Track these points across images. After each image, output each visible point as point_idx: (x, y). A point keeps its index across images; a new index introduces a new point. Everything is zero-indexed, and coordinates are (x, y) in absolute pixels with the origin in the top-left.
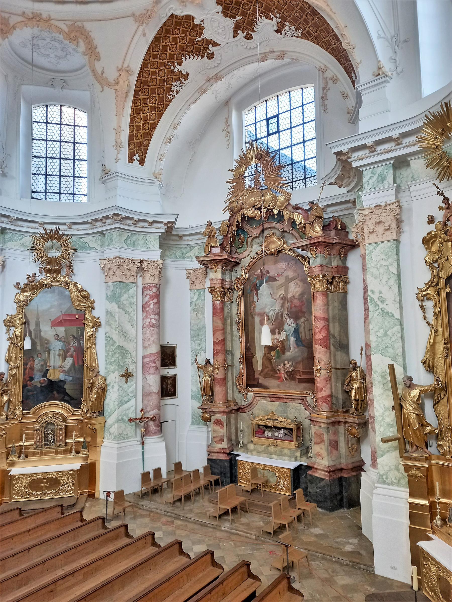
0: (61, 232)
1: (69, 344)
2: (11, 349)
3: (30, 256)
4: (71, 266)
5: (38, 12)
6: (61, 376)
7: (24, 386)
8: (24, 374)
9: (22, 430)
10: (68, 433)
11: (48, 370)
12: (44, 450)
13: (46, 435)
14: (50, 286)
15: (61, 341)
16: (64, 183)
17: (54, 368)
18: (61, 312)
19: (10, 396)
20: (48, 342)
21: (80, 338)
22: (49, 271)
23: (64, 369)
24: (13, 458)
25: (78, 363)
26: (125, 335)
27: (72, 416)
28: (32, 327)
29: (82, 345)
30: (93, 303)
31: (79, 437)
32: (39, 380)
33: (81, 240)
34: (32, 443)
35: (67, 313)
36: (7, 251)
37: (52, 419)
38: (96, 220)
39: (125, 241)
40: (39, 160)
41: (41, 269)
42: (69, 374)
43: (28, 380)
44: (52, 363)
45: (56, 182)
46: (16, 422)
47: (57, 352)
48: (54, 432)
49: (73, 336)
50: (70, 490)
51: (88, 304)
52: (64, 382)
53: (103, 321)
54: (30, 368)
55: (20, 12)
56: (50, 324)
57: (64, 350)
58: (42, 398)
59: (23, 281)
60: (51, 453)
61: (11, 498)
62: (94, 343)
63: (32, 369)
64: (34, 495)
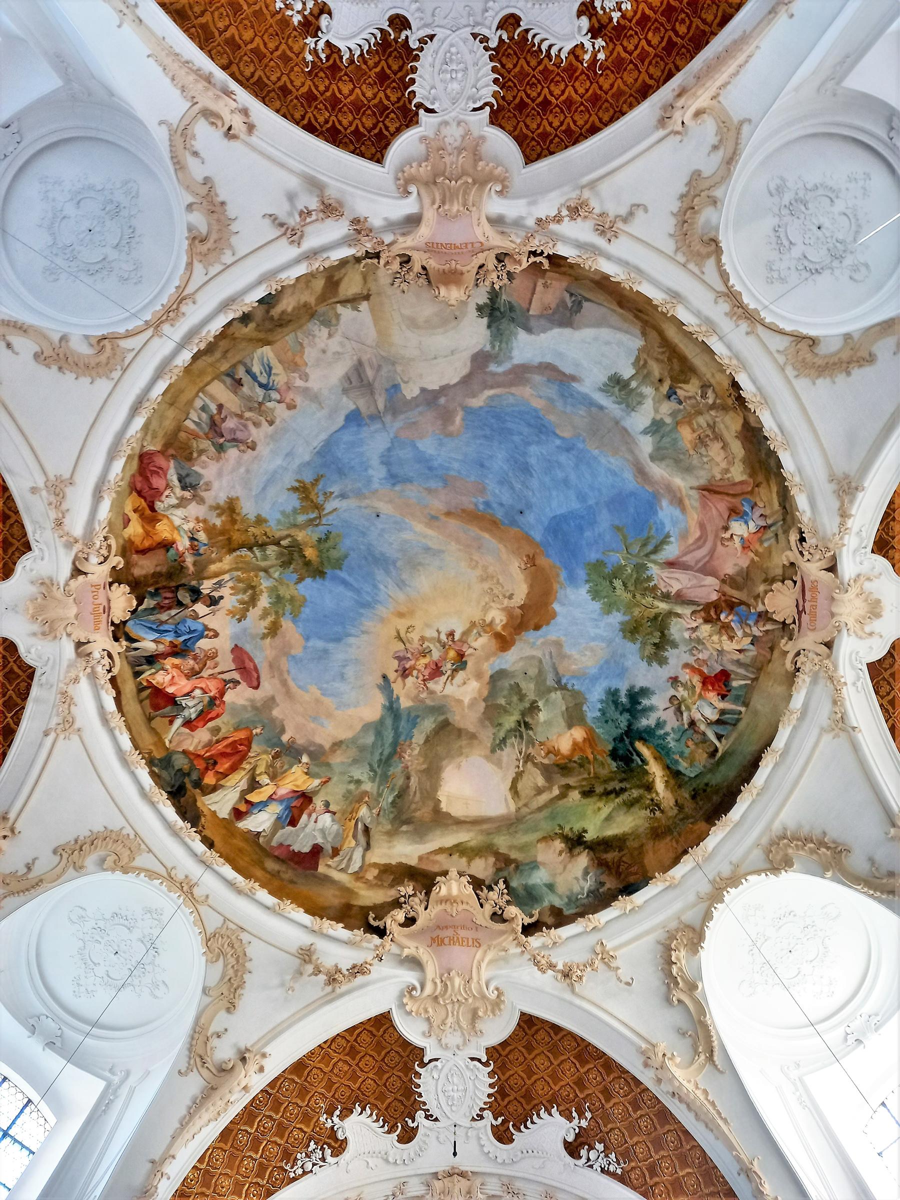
5: (178, 324)
55: (199, 297)
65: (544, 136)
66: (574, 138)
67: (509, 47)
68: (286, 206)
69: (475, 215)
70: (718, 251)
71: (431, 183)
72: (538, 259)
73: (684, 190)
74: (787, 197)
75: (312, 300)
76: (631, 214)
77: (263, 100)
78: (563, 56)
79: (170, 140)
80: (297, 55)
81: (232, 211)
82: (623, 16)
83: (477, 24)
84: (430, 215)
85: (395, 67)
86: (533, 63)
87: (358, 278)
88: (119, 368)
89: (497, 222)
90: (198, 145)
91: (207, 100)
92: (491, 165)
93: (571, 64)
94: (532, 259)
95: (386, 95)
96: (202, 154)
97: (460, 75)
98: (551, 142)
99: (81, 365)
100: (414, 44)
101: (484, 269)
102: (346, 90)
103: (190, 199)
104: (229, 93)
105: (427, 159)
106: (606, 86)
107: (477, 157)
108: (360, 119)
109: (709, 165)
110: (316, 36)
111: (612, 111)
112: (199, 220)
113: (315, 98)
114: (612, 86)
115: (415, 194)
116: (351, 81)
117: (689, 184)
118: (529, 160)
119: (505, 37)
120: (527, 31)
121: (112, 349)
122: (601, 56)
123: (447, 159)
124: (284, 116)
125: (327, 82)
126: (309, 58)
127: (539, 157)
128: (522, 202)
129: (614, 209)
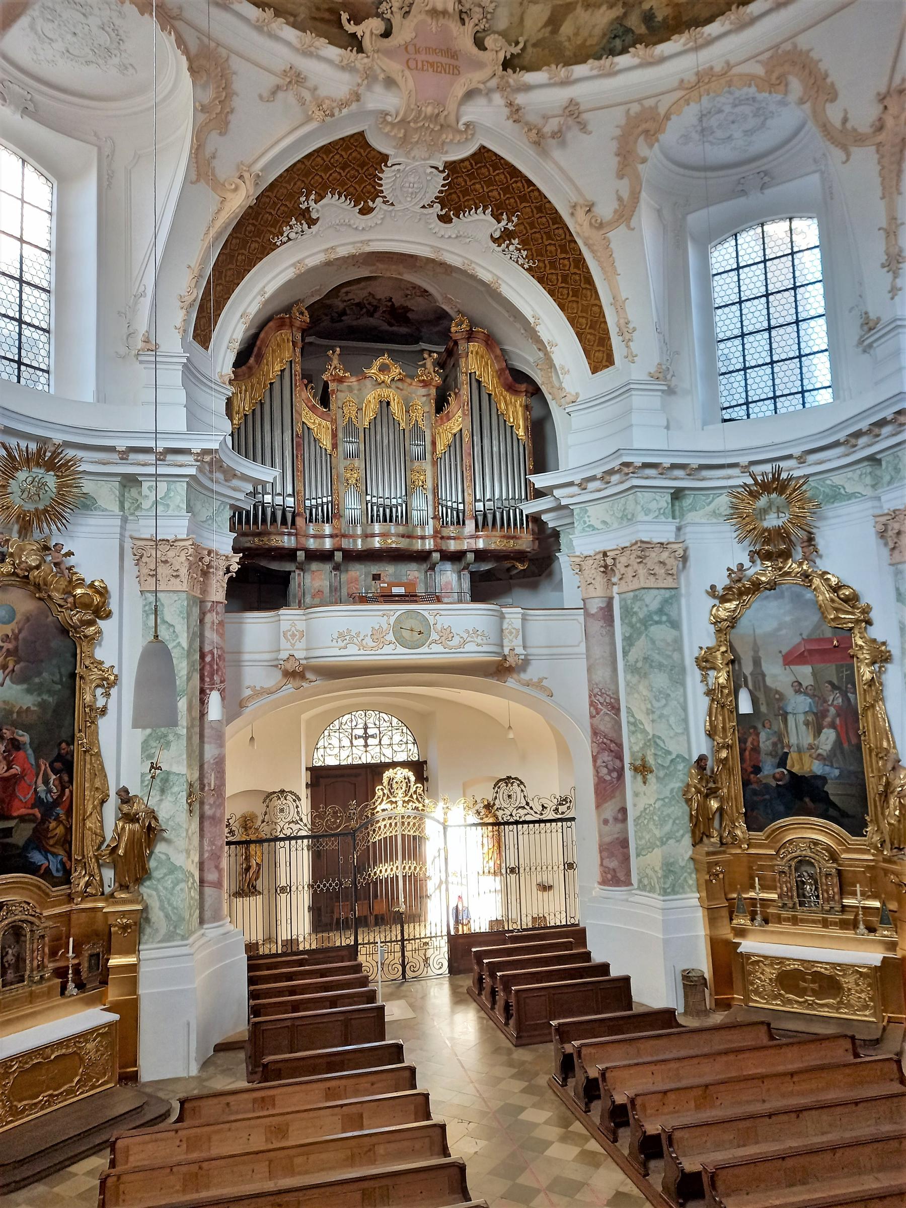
0: (784, 476)
1: (825, 701)
2: (714, 711)
3: (728, 533)
4: (810, 540)
6: (817, 768)
7: (746, 783)
8: (742, 760)
9: (751, 868)
10: (844, 886)
11: (786, 754)
12: (800, 915)
13: (800, 885)
14: (773, 586)
15: (806, 694)
16: (781, 375)
18: (801, 634)
19: (722, 800)
20: (782, 697)
21: (846, 687)
22: (768, 556)
23: (820, 751)
24: (742, 921)
25: (849, 742)
27: (848, 850)
28: (747, 669)
29: (852, 700)
30: (866, 610)
31: (868, 897)
32: (772, 772)
33: (828, 482)
34: (774, 896)
35: (814, 637)
36: (688, 529)
38: (858, 434)
40: (729, 344)
41: (752, 554)
42: (832, 763)
43: (752, 773)
44: (793, 740)
45: (765, 378)
46: (739, 851)
47: (801, 718)
48: (816, 883)
49: (831, 683)
50: (866, 1007)
51: (858, 615)
52: (823, 779)
53: (894, 648)
54: (752, 749)
56: (781, 661)
57: (815, 714)
58: (781, 808)
59: (722, 582)
60: (814, 922)
61: (747, 999)
62: (879, 697)
63: (756, 749)
64: (790, 1001)
66: (325, 149)
67: (368, 198)
68: (569, 136)
69: (413, 100)
70: (191, 69)
72: (351, 28)
73: (230, 117)
75: (579, 10)
76: (274, 93)
79: (632, 215)
80: (522, 223)
81: (614, 146)
82: (288, 224)
83: (390, 211)
84: (452, 106)
85: (454, 196)
86: (351, 189)
87: (528, 22)
88: (780, 51)
89: (390, 82)
90: (615, 205)
91: (596, 236)
92: (393, 134)
93: (324, 191)
94: (358, 30)
95: (466, 182)
98: (341, 146)
99: (807, 71)
100: (437, 206)
101: (404, 10)
102: (495, 193)
103: (640, 167)
104: (578, 233)
105: (443, 143)
108: (490, 174)
109: (214, 141)
112: (642, 149)
113: (519, 197)
115: (461, 123)
116: (489, 197)
117: (227, 123)
119: (370, 203)
120: (355, 206)
121: (773, 72)
122: (303, 199)
124: (546, 198)
125: (507, 202)
126: (515, 219)
129: (289, 97)
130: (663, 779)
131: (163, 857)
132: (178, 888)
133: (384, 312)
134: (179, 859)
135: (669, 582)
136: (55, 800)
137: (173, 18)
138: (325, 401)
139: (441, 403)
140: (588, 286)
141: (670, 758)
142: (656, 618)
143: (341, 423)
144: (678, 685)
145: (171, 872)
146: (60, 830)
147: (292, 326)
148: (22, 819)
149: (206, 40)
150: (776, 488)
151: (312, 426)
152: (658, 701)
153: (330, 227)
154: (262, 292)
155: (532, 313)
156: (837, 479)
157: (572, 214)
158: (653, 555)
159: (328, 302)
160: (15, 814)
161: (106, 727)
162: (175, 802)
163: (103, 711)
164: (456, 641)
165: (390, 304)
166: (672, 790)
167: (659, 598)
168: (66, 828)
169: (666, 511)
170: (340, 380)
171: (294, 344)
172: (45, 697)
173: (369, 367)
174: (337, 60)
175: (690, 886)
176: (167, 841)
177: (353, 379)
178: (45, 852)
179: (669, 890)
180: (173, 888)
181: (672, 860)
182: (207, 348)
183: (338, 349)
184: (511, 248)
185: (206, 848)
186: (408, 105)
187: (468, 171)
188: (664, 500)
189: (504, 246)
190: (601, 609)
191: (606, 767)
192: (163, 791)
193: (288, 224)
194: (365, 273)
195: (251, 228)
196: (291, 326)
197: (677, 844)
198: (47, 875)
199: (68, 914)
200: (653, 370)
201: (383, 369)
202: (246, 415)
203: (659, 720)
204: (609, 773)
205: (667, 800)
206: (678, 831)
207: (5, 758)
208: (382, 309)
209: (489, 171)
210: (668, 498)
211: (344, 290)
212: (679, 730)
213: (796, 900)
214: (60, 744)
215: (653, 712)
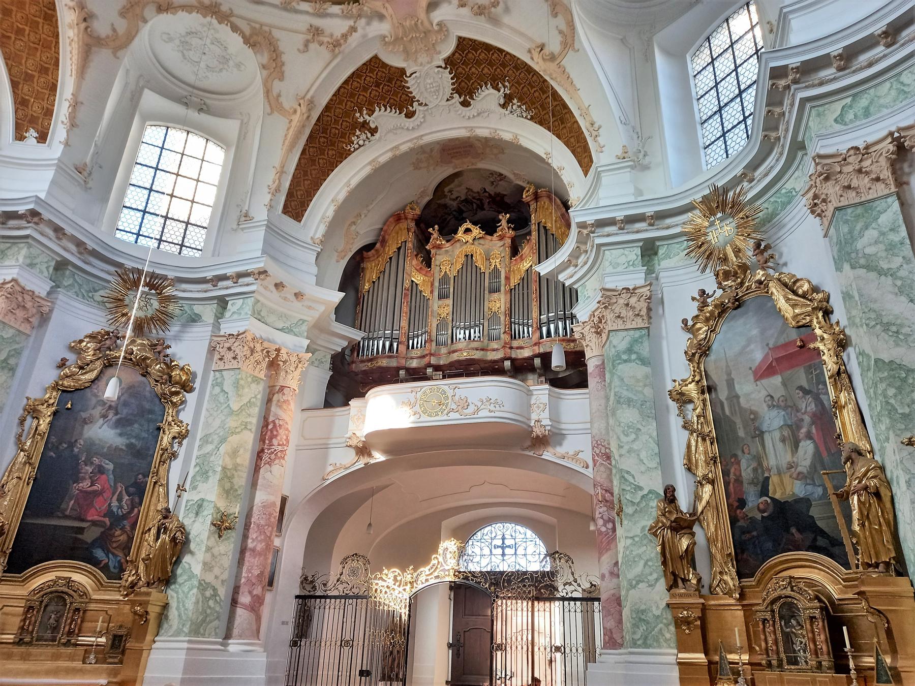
1: (798, 411)
6: (797, 489)
7: (734, 521)
15: (778, 407)
17: (779, 473)
18: (767, 345)
21: (818, 389)
22: (727, 275)
25: (828, 450)
26: (894, 329)
35: (779, 343)
36: (661, 275)
37: (788, 592)
39: (840, 120)
42: (813, 480)
43: (738, 507)
44: (772, 462)
47: (777, 435)
49: (801, 388)
56: (751, 377)
57: (790, 426)
58: (769, 545)
63: (739, 480)
65: (371, 71)
69: (395, 21)
71: (427, 33)
73: (284, 68)
74: (231, 63)
77: (526, 64)
78: (377, 109)
79: (574, 40)
80: (513, 85)
82: (354, 134)
83: (427, 110)
84: (422, 15)
85: (463, 84)
86: (392, 101)
89: (381, 17)
91: (552, 66)
96: (557, 32)
97: (428, 86)
98: (367, 69)
102: (486, 70)
105: (433, 45)
106: (349, 103)
107: (406, 52)
109: (277, 86)
110: (505, 94)
111: (340, 93)
114: (346, 105)
117: (283, 73)
118: (376, 57)
119: (411, 108)
120: (400, 113)
122: (358, 115)
123: (422, 46)
124: (515, 56)
126: (507, 84)
127: (370, 60)
128: (370, 35)
130: (633, 515)
131: (187, 566)
132: (191, 593)
133: (489, 203)
134: (197, 569)
135: (639, 323)
136: (124, 515)
137: (228, 16)
138: (429, 265)
139: (515, 251)
140: (566, 111)
141: (640, 493)
142: (625, 357)
143: (437, 277)
144: (650, 420)
145: (190, 579)
146: (123, 538)
147: (406, 219)
148: (94, 523)
149: (253, 24)
150: (717, 207)
151: (418, 283)
152: (627, 435)
153: (388, 132)
154: (348, 184)
155: (544, 151)
156: (789, 186)
157: (532, 59)
158: (621, 301)
159: (442, 201)
160: (89, 519)
161: (176, 466)
162: (203, 523)
163: (174, 455)
164: (471, 409)
165: (487, 194)
166: (643, 528)
167: (628, 339)
168: (128, 536)
169: (636, 262)
170: (439, 247)
171: (408, 230)
172: (133, 441)
173: (456, 232)
174: (339, 12)
175: (666, 640)
176: (192, 553)
177: (448, 245)
178: (107, 552)
179: (639, 642)
180: (188, 592)
181: (643, 607)
182: (300, 221)
183: (436, 226)
184: (514, 107)
185: (244, 574)
186: (393, 24)
187: (461, 61)
188: (634, 253)
189: (509, 108)
190: (597, 366)
191: (602, 518)
192: (197, 514)
193: (354, 134)
194: (447, 171)
195: (322, 140)
196: (406, 219)
197: (650, 589)
198: (105, 569)
199: (117, 602)
200: (619, 153)
201: (467, 231)
202: (374, 282)
203: (628, 455)
204: (604, 525)
205: (637, 539)
206: (651, 574)
207: (91, 478)
208: (486, 201)
209: (473, 54)
210: (639, 251)
211: (446, 189)
212: (653, 464)
213: (783, 655)
214: (138, 475)
215: (622, 447)
